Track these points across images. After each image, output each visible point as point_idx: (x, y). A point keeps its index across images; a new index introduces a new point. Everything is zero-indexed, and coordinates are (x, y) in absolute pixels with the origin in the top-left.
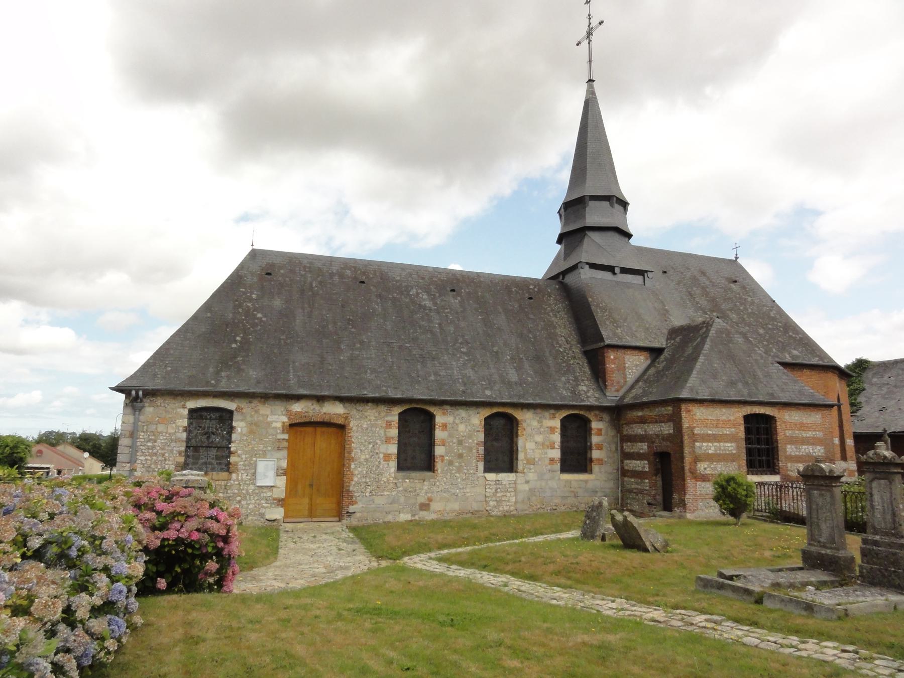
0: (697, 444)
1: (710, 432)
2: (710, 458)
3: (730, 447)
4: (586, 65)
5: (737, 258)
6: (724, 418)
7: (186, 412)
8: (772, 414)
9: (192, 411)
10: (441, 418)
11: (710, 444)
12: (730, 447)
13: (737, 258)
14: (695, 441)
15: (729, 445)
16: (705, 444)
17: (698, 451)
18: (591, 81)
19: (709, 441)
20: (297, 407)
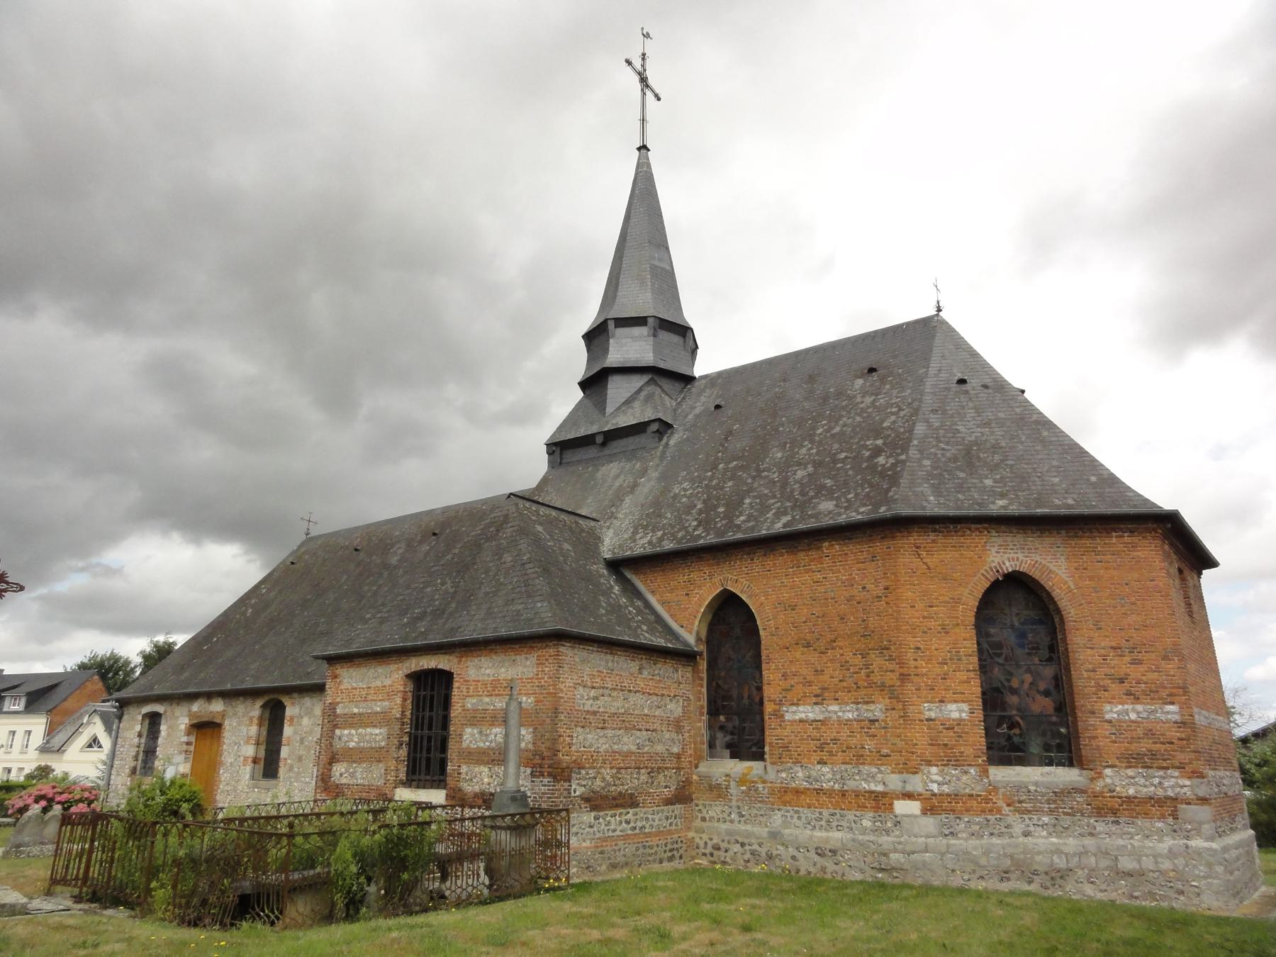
0: (338, 732)
1: (356, 710)
2: (601, 722)
3: (377, 735)
4: (638, 124)
5: (939, 310)
6: (378, 683)
7: (140, 718)
8: (447, 668)
9: (145, 716)
10: (286, 701)
11: (353, 732)
12: (377, 735)
13: (939, 310)
14: (336, 726)
15: (377, 731)
16: (346, 732)
17: (338, 745)
18: (643, 148)
19: (351, 726)
20: (196, 707)
